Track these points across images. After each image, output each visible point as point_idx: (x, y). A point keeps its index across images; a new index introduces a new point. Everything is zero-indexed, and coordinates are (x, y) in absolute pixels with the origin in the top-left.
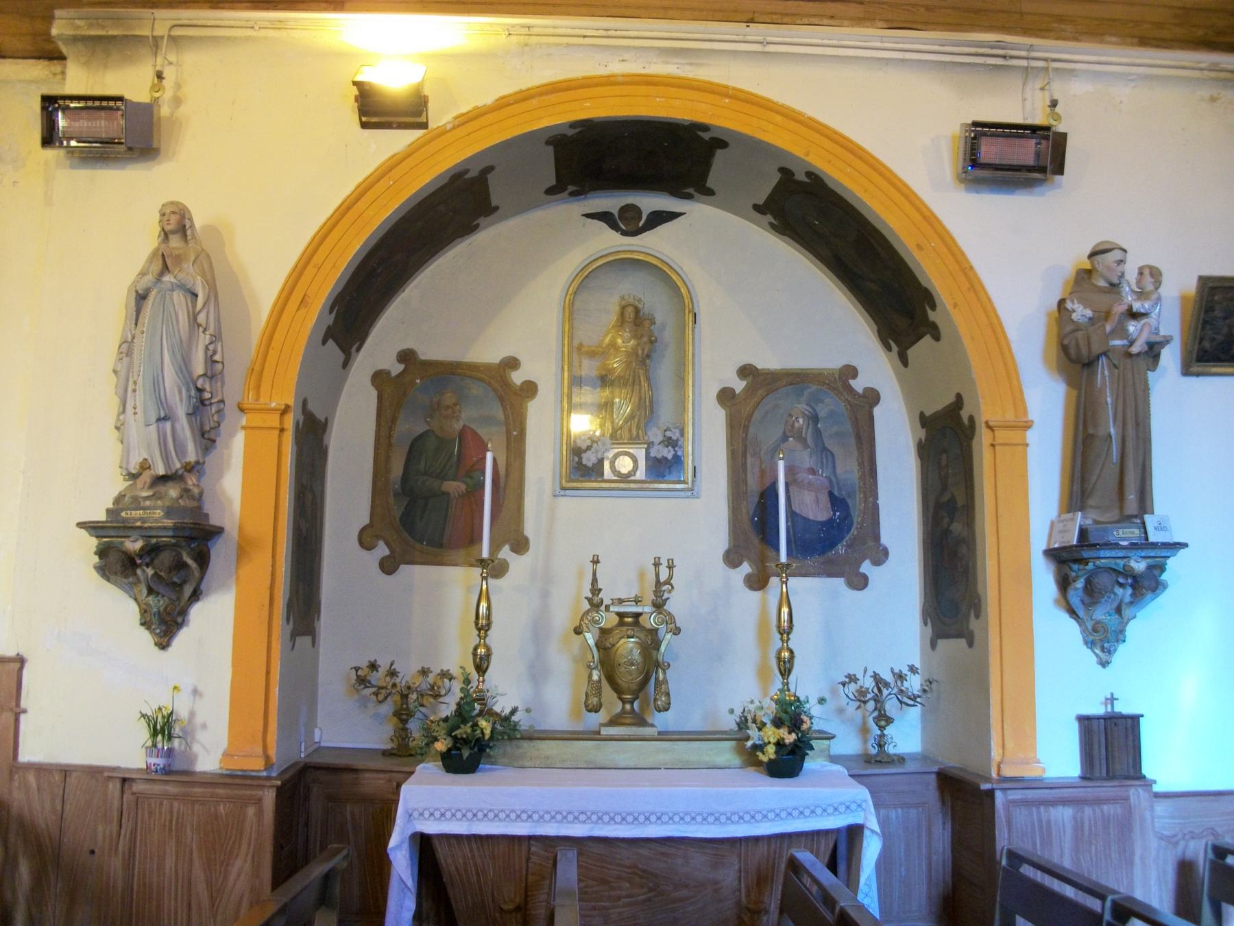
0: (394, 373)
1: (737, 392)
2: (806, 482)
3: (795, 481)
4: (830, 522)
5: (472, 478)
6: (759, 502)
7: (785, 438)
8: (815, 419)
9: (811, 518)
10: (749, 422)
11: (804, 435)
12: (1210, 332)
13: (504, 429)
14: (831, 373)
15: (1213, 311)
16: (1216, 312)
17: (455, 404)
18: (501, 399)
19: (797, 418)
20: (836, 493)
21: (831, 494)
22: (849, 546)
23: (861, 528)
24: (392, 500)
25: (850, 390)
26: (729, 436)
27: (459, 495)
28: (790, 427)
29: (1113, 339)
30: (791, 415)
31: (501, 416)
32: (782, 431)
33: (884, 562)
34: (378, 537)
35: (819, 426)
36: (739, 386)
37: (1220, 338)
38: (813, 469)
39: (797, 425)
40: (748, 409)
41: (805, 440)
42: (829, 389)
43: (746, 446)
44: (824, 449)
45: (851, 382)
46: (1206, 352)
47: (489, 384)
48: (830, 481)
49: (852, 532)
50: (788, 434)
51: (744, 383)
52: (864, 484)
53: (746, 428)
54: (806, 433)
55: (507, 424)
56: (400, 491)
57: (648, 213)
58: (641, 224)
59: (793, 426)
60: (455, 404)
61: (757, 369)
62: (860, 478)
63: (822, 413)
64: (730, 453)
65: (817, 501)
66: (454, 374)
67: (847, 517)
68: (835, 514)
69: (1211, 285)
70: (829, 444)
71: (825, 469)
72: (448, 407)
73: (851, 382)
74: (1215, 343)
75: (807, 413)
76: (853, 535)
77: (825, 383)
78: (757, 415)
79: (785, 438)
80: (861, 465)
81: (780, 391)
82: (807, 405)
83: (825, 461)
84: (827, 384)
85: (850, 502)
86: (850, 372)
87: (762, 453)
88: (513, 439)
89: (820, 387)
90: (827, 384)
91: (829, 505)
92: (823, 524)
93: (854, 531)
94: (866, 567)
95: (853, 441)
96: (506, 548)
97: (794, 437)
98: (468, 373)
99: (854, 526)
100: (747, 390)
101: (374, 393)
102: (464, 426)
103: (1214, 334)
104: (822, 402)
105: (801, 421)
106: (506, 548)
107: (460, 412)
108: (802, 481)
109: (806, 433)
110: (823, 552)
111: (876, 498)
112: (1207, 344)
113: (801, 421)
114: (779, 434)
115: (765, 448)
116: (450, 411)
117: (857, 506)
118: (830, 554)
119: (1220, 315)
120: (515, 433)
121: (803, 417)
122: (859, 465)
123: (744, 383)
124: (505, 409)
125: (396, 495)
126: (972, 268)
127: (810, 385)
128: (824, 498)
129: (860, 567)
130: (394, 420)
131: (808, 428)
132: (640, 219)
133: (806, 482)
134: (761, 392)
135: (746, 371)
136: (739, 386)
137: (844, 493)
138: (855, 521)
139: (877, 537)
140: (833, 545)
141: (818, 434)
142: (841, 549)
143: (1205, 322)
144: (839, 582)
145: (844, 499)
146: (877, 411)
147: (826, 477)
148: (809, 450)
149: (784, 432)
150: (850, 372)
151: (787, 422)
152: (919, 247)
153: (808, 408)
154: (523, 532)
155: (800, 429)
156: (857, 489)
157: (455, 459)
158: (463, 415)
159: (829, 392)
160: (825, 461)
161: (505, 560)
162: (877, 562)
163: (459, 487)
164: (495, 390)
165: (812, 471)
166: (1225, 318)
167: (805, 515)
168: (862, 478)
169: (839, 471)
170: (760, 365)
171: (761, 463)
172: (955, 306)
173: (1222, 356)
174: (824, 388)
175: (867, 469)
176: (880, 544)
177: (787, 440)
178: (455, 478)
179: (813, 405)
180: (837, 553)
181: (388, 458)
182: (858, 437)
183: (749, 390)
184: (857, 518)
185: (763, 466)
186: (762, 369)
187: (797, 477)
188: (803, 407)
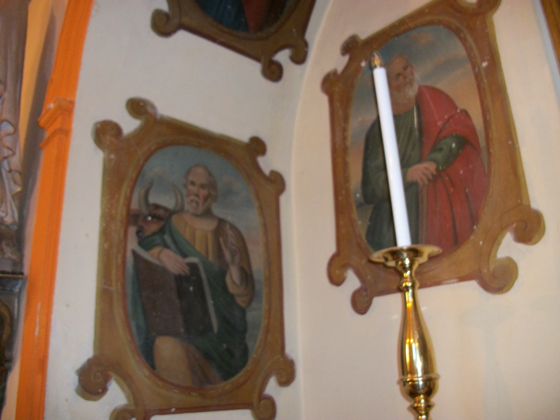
0: (340, 69)
5: (441, 150)
13: (469, 66)
17: (405, 68)
18: (457, 32)
24: (355, 215)
27: (429, 180)
31: (461, 51)
34: (345, 266)
47: (440, 23)
55: (471, 58)
56: (362, 200)
60: (405, 68)
66: (398, 35)
72: (399, 75)
88: (483, 74)
96: (508, 238)
98: (411, 25)
101: (325, 99)
102: (420, 88)
106: (508, 238)
107: (412, 74)
116: (401, 78)
120: (485, 64)
124: (464, 41)
125: (360, 206)
130: (346, 119)
154: (529, 206)
157: (417, 133)
158: (417, 76)
161: (509, 259)
163: (427, 169)
164: (448, 26)
178: (420, 161)
181: (345, 164)
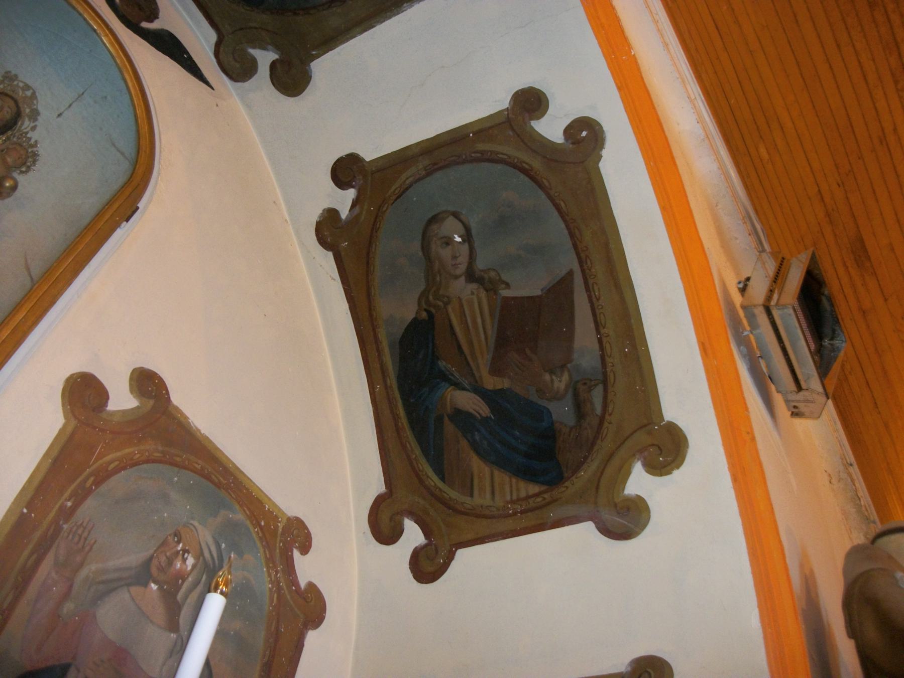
1: (112, 406)
10: (98, 483)
11: (179, 597)
19: (185, 551)
26: (36, 483)
28: (163, 559)
30: (178, 535)
32: (143, 555)
42: (260, 539)
43: (58, 530)
45: (296, 554)
50: (154, 570)
53: (81, 497)
57: (166, 28)
58: (144, 25)
59: (170, 562)
64: (13, 519)
77: (260, 525)
78: (119, 484)
82: (214, 538)
84: (261, 528)
87: (84, 573)
89: (248, 523)
90: (261, 528)
97: (160, 588)
105: (190, 561)
109: (186, 597)
113: (190, 561)
114: (132, 559)
115: (93, 567)
121: (197, 558)
127: (237, 507)
132: (151, 20)
134: (151, 447)
146: (312, 638)
148: (173, 636)
151: (164, 543)
153: (213, 549)
155: (182, 576)
159: (259, 544)
170: (177, 398)
171: (66, 596)
174: (254, 531)
177: (146, 585)
179: (223, 545)
186: (176, 408)
188: (205, 535)
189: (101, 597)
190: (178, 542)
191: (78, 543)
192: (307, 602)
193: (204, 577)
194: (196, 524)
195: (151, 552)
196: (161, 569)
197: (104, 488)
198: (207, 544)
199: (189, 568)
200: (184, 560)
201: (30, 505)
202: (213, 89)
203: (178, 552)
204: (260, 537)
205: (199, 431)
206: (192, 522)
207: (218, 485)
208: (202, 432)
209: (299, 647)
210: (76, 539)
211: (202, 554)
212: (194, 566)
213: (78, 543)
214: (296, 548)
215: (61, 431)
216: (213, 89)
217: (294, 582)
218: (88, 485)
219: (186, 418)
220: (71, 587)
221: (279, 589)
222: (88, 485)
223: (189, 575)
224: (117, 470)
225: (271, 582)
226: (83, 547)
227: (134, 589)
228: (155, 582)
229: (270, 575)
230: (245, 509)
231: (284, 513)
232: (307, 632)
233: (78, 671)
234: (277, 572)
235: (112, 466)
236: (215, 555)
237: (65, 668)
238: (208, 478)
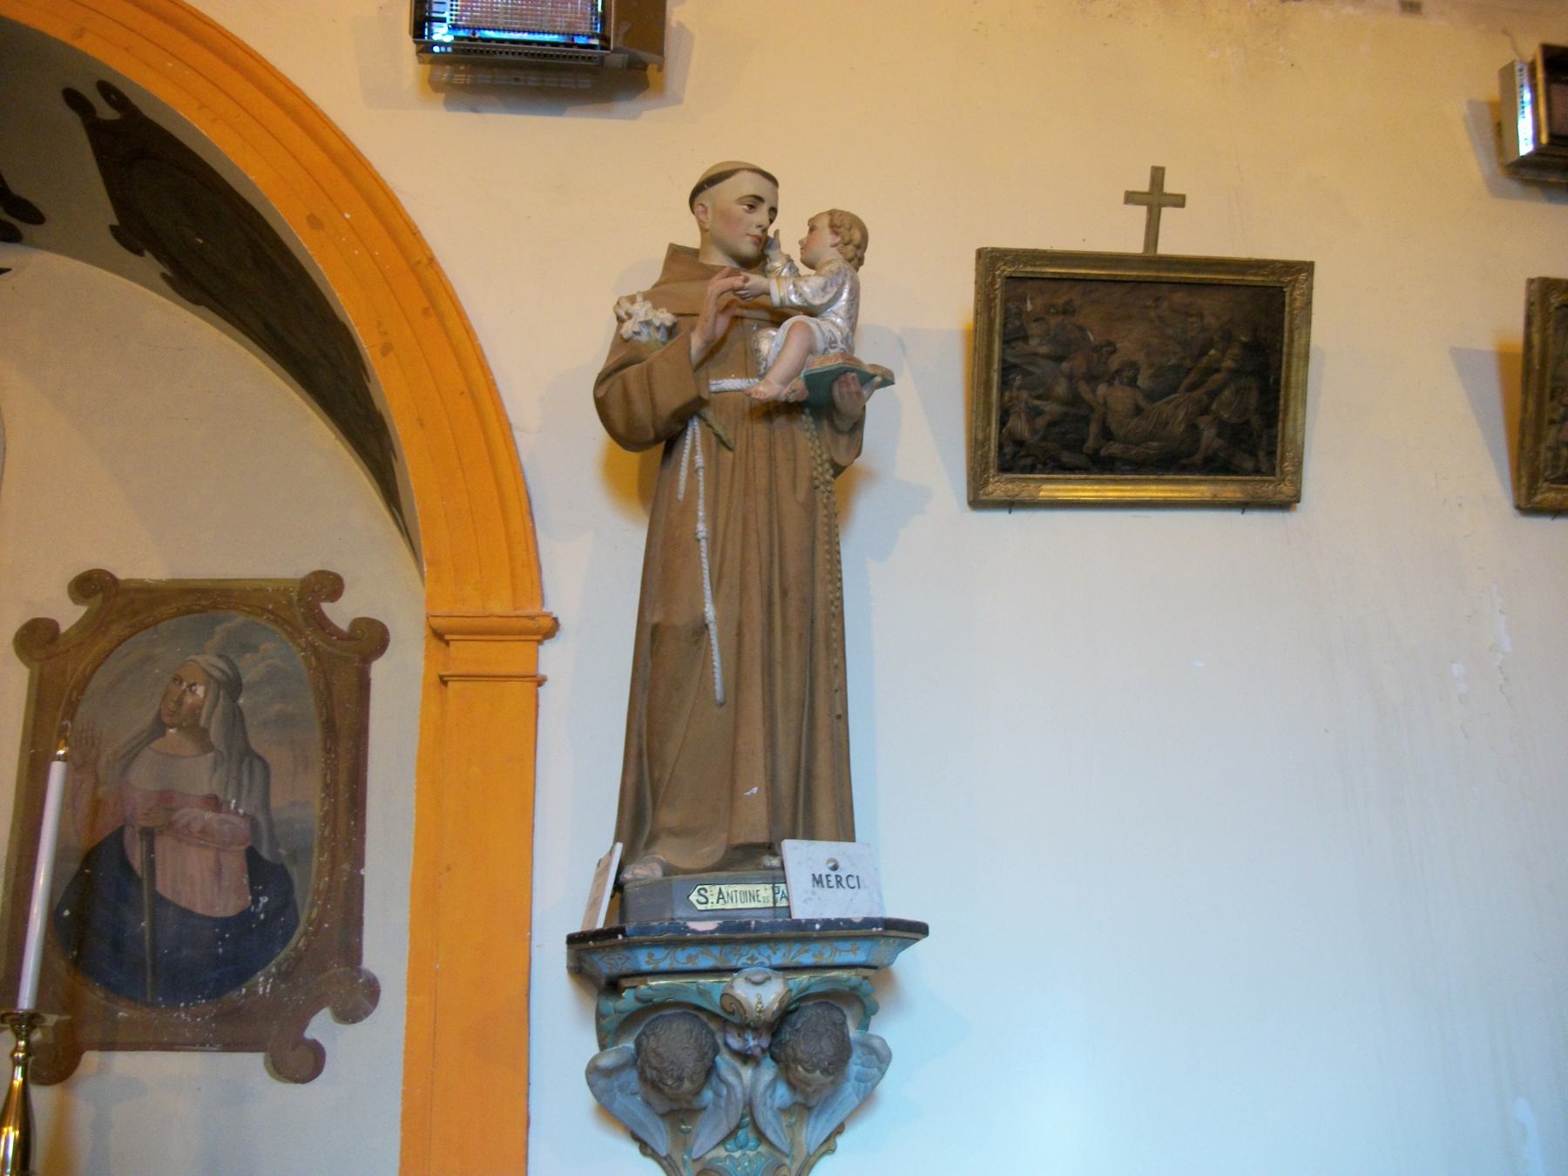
1: (64, 628)
2: (196, 827)
3: (170, 825)
4: (245, 917)
6: (80, 872)
7: (159, 728)
8: (233, 686)
9: (199, 909)
10: (82, 692)
11: (202, 722)
12: (1024, 394)
14: (282, 587)
15: (1025, 339)
16: (1034, 342)
19: (190, 686)
20: (265, 853)
21: (252, 856)
22: (283, 976)
23: (316, 933)
25: (322, 623)
28: (172, 705)
29: (725, 375)
30: (178, 680)
33: (367, 1013)
35: (241, 701)
36: (68, 615)
37: (1051, 408)
38: (216, 798)
39: (189, 700)
40: (81, 667)
41: (205, 731)
42: (275, 622)
44: (247, 752)
45: (326, 607)
46: (1020, 443)
48: (254, 825)
49: (293, 942)
50: (166, 720)
51: (82, 610)
52: (334, 830)
54: (209, 718)
59: (180, 702)
61: (115, 581)
62: (325, 819)
63: (251, 671)
65: (218, 873)
67: (285, 906)
68: (255, 902)
69: (1008, 270)
70: (259, 741)
71: (244, 793)
73: (326, 607)
74: (1041, 422)
75: (216, 673)
76: (296, 949)
77: (265, 610)
78: (100, 680)
79: (159, 728)
80: (329, 789)
81: (162, 626)
82: (220, 656)
83: (245, 781)
85: (294, 872)
86: (330, 585)
89: (251, 618)
91: (245, 881)
92: (225, 923)
93: (298, 940)
94: (321, 1026)
95: (315, 735)
97: (179, 727)
99: (301, 929)
100: (80, 625)
103: (1038, 397)
104: (254, 648)
105: (200, 690)
108: (188, 825)
109: (209, 718)
110: (218, 991)
111: (359, 860)
112: (1019, 425)
113: (200, 690)
117: (309, 883)
118: (234, 995)
119: (1044, 350)
121: (207, 684)
122: (326, 786)
123: (82, 610)
126: (432, 260)
128: (235, 864)
129: (306, 1026)
131: (215, 705)
133: (196, 827)
134: (116, 630)
135: (89, 585)
136: (68, 615)
137: (283, 852)
138: (303, 918)
139: (352, 952)
140: (243, 975)
141: (236, 719)
142: (262, 984)
143: (1007, 369)
144: (253, 1064)
145: (282, 866)
146: (379, 670)
147: (245, 815)
148: (211, 755)
149: (158, 717)
150: (330, 585)
152: (314, 222)
153: (222, 665)
155: (195, 710)
156: (316, 842)
159: (273, 627)
160: (245, 781)
162: (350, 1014)
165: (214, 803)
166: (1059, 359)
167: (184, 904)
168: (330, 818)
169: (276, 802)
171: (96, 786)
172: (386, 349)
173: (1066, 457)
175: (344, 796)
176: (359, 972)
177: (163, 734)
179: (232, 657)
180: (252, 992)
182: (330, 728)
183: (91, 627)
184: (307, 913)
185: (101, 791)
187: (176, 816)
188: (209, 660)
189: (126, 769)
190: (181, 683)
191: (87, 743)
192: (360, 639)
193: (221, 693)
194: (192, 657)
195: (157, 707)
196: (173, 714)
197: (88, 692)
198: (213, 666)
199: (202, 696)
200: (194, 693)
201: (34, 744)
202: (8, 270)
203: (184, 691)
204: (273, 621)
205: (161, 581)
206: (188, 658)
207: (203, 610)
208: (164, 579)
209: (364, 686)
210: (84, 741)
211: (211, 676)
212: (206, 692)
213: (87, 743)
214: (324, 600)
215: (31, 678)
216: (8, 270)
217: (337, 631)
218: (73, 699)
219: (141, 581)
220: (97, 778)
221: (315, 649)
222: (73, 699)
223: (203, 702)
224: (93, 671)
225: (304, 650)
226: (93, 744)
227: (157, 744)
228: (171, 727)
229: (299, 645)
230: (243, 608)
231: (294, 581)
232: (370, 667)
233: (133, 827)
234: (306, 638)
235: (88, 671)
236: (226, 668)
237: (119, 834)
238: (189, 611)
